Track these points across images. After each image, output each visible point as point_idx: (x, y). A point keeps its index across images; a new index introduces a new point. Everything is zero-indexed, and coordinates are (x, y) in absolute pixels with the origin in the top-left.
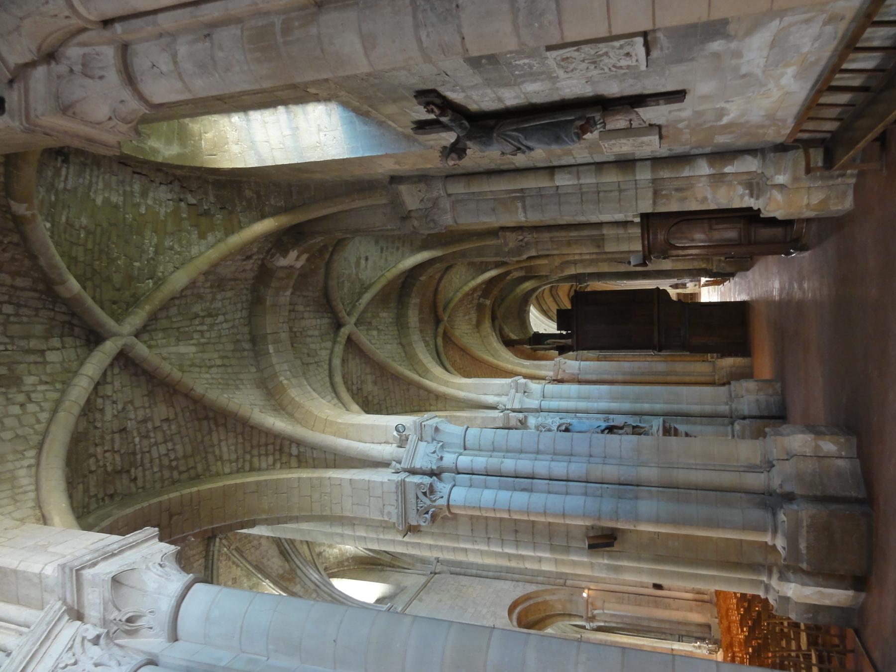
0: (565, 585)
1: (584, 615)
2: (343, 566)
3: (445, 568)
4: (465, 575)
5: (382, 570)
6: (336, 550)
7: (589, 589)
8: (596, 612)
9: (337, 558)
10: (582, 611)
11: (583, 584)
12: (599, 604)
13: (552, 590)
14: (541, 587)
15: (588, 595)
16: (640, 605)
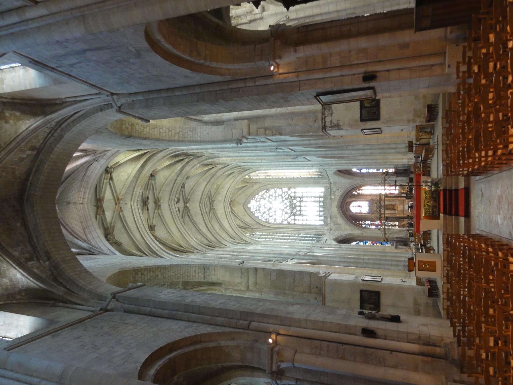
0: (248, 328)
1: (267, 368)
2: (14, 298)
3: (119, 305)
4: (139, 313)
5: (54, 306)
6: (6, 281)
7: (278, 334)
8: (283, 365)
9: (7, 289)
10: (265, 362)
11: (271, 327)
12: (288, 354)
13: (231, 332)
14: (219, 330)
15: (275, 342)
16: (343, 358)
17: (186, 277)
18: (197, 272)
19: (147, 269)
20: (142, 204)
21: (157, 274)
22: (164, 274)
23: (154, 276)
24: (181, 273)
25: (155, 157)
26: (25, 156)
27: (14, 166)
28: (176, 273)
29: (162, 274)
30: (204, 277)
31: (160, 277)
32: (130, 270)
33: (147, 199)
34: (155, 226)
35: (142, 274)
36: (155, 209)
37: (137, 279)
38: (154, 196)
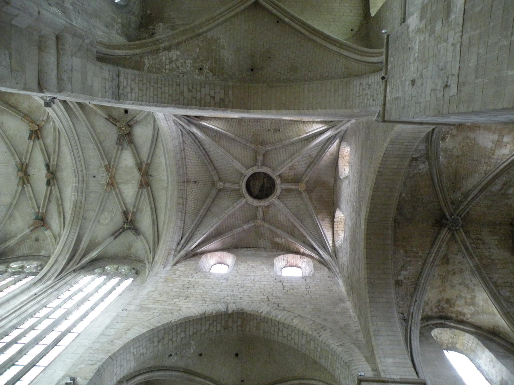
17: (145, 81)
18: (129, 89)
19: (205, 106)
20: (59, 175)
21: (190, 94)
22: (178, 91)
23: (194, 91)
24: (152, 88)
25: (67, 256)
26: (402, 273)
27: (408, 259)
28: (160, 91)
29: (182, 93)
30: (118, 76)
31: (186, 87)
32: (232, 108)
33: (51, 181)
34: (30, 138)
35: (214, 98)
36: (27, 165)
37: (222, 92)
38: (31, 186)
